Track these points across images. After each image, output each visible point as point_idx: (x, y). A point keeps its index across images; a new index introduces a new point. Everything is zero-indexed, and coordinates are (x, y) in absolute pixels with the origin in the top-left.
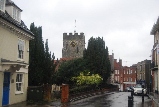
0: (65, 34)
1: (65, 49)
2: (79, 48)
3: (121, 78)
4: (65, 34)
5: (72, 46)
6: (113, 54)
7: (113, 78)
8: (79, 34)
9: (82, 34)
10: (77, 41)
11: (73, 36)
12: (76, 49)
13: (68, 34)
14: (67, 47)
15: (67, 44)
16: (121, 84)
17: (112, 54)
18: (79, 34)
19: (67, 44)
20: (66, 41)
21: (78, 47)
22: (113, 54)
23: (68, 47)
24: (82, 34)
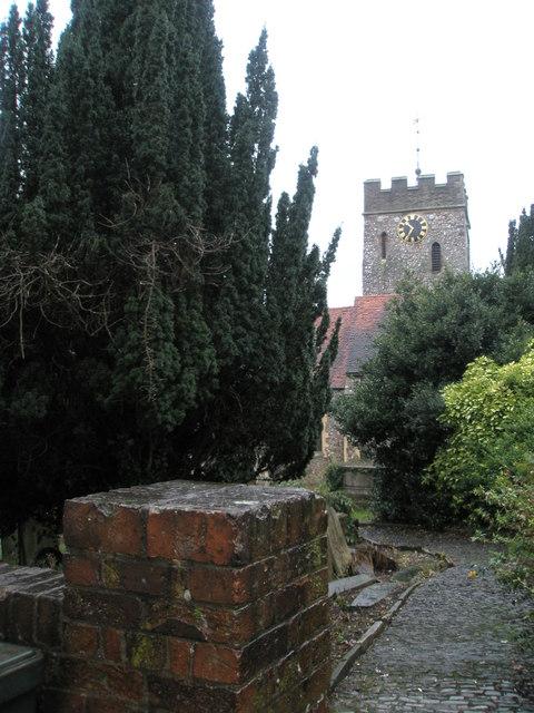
2: (445, 248)
4: (372, 187)
5: (410, 240)
8: (441, 180)
9: (455, 179)
10: (431, 216)
11: (413, 190)
12: (427, 251)
13: (386, 185)
14: (383, 245)
15: (384, 235)
18: (441, 180)
19: (384, 235)
20: (380, 218)
23: (391, 244)
24: (455, 179)
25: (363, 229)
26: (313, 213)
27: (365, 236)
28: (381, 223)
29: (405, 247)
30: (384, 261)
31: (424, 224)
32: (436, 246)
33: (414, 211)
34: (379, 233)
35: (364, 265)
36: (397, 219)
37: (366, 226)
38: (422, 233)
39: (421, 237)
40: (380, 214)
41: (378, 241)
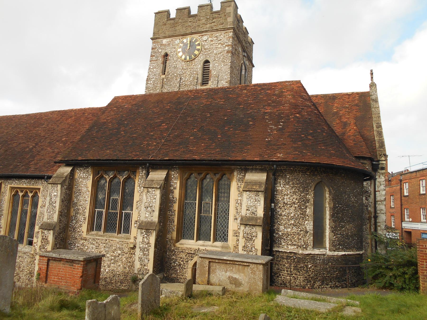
0: (162, 16)
3: (391, 208)
6: (373, 85)
7: (378, 198)
10: (205, 38)
14: (165, 63)
15: (166, 55)
16: (391, 228)
17: (366, 89)
20: (165, 41)
21: (207, 62)
22: (373, 85)
25: (150, 50)
26: (5, 115)
27: (152, 56)
28: (165, 45)
30: (164, 76)
31: (199, 45)
33: (192, 34)
34: (163, 54)
35: (147, 80)
36: (177, 41)
37: (152, 49)
38: (196, 52)
39: (195, 55)
40: (165, 37)
41: (161, 60)
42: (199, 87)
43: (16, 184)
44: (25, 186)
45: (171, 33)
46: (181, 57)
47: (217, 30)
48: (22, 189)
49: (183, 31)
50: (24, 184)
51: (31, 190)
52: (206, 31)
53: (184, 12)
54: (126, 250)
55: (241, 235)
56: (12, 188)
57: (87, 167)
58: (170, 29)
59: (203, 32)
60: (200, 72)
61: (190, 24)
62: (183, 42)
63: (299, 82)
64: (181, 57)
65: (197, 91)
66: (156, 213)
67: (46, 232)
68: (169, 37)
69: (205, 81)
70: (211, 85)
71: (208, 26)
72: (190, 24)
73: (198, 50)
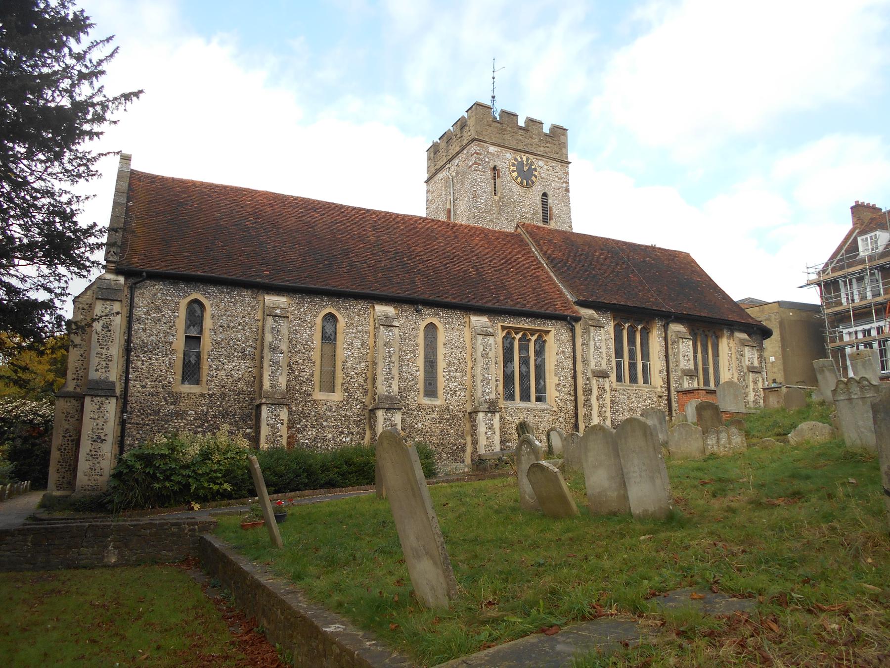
1: (490, 188)
5: (522, 183)
9: (558, 133)
10: (541, 163)
15: (495, 168)
19: (495, 168)
20: (492, 149)
24: (558, 133)
28: (493, 155)
29: (517, 189)
30: (497, 198)
32: (545, 195)
34: (491, 165)
38: (533, 178)
39: (533, 183)
40: (493, 144)
41: (490, 174)
42: (541, 224)
43: (510, 322)
44: (526, 326)
45: (500, 141)
46: (516, 178)
47: (554, 159)
48: (517, 330)
49: (513, 144)
50: (525, 324)
51: (533, 332)
52: (543, 156)
53: (510, 116)
54: (655, 399)
55: (751, 379)
56: (503, 328)
57: (606, 312)
58: (498, 135)
59: (539, 155)
60: (540, 205)
61: (521, 138)
62: (516, 160)
63: (688, 255)
64: (516, 178)
65: (537, 227)
66: (692, 362)
67: (600, 379)
68: (499, 146)
69: (545, 220)
70: (552, 225)
71: (542, 149)
72: (521, 138)
73: (536, 177)
